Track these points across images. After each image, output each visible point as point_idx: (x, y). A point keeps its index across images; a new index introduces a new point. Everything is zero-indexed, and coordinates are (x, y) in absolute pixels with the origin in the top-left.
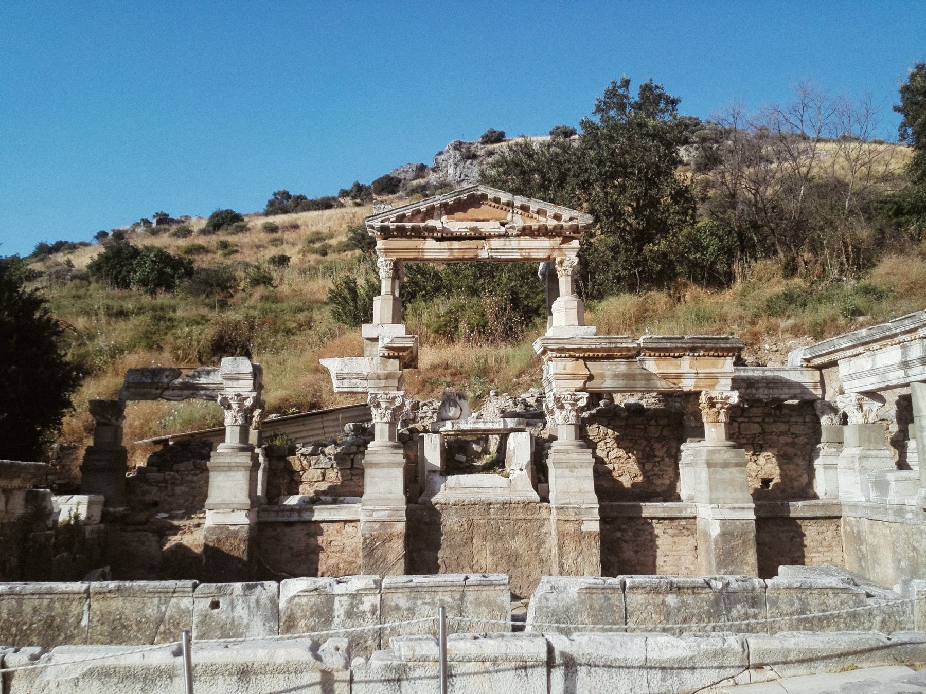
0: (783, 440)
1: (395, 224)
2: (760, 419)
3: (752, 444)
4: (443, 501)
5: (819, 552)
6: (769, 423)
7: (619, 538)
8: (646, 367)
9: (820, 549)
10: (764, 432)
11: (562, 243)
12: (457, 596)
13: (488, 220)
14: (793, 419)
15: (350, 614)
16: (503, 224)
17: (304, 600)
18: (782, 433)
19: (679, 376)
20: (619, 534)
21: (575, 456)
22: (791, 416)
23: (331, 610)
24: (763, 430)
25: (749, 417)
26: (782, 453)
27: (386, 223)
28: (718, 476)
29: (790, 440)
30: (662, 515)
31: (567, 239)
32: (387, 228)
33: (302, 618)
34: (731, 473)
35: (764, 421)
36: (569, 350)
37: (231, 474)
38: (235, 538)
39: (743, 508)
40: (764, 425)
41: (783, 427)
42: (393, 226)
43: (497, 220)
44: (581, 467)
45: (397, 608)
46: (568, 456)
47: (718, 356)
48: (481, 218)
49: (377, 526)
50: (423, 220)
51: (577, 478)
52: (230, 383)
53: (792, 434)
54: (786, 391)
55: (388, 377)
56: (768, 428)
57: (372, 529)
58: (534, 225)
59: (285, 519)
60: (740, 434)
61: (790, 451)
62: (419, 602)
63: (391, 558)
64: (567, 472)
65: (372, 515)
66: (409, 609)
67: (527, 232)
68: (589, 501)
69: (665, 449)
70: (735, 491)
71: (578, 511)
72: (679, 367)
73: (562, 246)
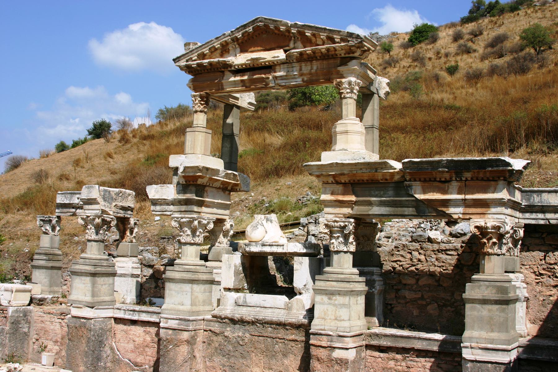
1: (195, 62)
7: (390, 368)
11: (341, 65)
20: (392, 363)
21: (334, 284)
28: (475, 313)
34: (489, 311)
36: (334, 176)
38: (85, 327)
42: (194, 64)
47: (488, 180)
49: (170, 332)
50: (222, 56)
51: (334, 305)
52: (86, 207)
55: (187, 202)
57: (167, 334)
63: (180, 359)
65: (167, 323)
67: (305, 57)
68: (342, 329)
70: (492, 331)
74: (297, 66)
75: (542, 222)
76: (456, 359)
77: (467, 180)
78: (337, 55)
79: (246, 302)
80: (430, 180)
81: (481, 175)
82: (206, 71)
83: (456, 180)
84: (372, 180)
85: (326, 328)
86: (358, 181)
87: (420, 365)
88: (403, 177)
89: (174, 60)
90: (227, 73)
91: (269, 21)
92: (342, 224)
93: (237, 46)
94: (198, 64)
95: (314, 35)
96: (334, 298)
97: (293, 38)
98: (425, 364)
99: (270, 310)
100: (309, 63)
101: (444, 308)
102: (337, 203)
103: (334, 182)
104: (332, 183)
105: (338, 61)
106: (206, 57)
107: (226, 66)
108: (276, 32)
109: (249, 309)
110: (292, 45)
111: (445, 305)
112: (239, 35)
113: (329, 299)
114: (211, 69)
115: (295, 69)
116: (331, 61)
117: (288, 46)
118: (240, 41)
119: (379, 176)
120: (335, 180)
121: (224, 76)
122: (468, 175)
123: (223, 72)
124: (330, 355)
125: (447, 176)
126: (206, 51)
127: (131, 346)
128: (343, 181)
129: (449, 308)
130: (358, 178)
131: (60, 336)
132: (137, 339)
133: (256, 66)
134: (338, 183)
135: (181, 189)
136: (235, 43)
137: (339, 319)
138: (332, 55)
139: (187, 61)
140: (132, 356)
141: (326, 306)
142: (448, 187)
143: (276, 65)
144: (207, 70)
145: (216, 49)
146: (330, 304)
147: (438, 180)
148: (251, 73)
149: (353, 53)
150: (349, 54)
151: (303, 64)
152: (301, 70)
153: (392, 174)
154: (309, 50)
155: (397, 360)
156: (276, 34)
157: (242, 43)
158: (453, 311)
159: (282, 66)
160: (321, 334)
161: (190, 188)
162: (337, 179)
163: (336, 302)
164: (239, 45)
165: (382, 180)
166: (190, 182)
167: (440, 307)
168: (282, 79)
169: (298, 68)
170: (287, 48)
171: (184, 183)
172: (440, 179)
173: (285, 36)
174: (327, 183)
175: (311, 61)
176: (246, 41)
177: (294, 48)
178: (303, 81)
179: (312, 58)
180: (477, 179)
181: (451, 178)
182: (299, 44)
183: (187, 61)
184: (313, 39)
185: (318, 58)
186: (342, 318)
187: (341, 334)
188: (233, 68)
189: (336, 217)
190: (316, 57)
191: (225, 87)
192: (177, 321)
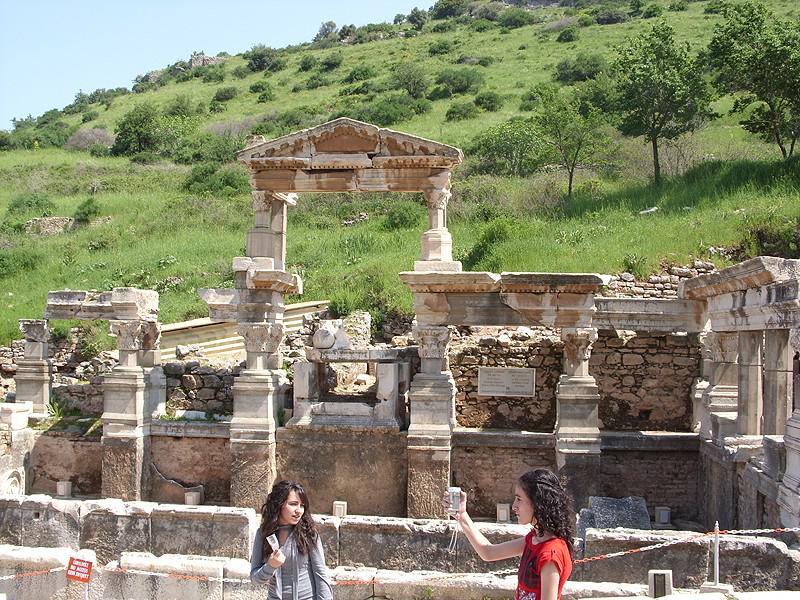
1: (264, 159)
2: (644, 350)
3: (633, 375)
5: (674, 484)
6: (653, 355)
8: (508, 303)
9: (674, 481)
10: (646, 363)
12: (208, 524)
13: (356, 152)
15: (129, 530)
17: (97, 517)
18: (666, 365)
19: (539, 313)
20: (479, 462)
22: (676, 347)
23: (115, 527)
24: (645, 361)
25: (633, 348)
26: (662, 384)
29: (672, 372)
30: (522, 446)
31: (437, 171)
33: (95, 530)
34: (581, 409)
35: (647, 352)
36: (429, 286)
37: (122, 394)
41: (665, 358)
44: (437, 401)
45: (163, 529)
48: (349, 150)
50: (293, 153)
53: (675, 365)
54: (669, 323)
56: (650, 359)
59: (173, 434)
60: (622, 365)
61: (670, 382)
62: (180, 526)
64: (422, 405)
66: (172, 531)
69: (545, 379)
72: (539, 303)
73: (430, 179)
74: (383, 172)
75: (607, 328)
81: (574, 289)
90: (300, 174)
94: (267, 162)
95: (404, 143)
107: (300, 165)
109: (329, 418)
110: (377, 151)
116: (421, 171)
119: (476, 287)
122: (562, 288)
124: (430, 458)
125: (542, 289)
127: (176, 465)
131: (74, 461)
132: (183, 458)
133: (336, 168)
134: (431, 292)
139: (252, 157)
140: (178, 475)
151: (390, 171)
152: (387, 177)
153: (489, 286)
154: (401, 159)
155: (484, 459)
160: (419, 439)
161: (260, 292)
178: (389, 187)
182: (386, 150)
183: (252, 157)
188: (309, 168)
189: (429, 325)
192: (252, 435)
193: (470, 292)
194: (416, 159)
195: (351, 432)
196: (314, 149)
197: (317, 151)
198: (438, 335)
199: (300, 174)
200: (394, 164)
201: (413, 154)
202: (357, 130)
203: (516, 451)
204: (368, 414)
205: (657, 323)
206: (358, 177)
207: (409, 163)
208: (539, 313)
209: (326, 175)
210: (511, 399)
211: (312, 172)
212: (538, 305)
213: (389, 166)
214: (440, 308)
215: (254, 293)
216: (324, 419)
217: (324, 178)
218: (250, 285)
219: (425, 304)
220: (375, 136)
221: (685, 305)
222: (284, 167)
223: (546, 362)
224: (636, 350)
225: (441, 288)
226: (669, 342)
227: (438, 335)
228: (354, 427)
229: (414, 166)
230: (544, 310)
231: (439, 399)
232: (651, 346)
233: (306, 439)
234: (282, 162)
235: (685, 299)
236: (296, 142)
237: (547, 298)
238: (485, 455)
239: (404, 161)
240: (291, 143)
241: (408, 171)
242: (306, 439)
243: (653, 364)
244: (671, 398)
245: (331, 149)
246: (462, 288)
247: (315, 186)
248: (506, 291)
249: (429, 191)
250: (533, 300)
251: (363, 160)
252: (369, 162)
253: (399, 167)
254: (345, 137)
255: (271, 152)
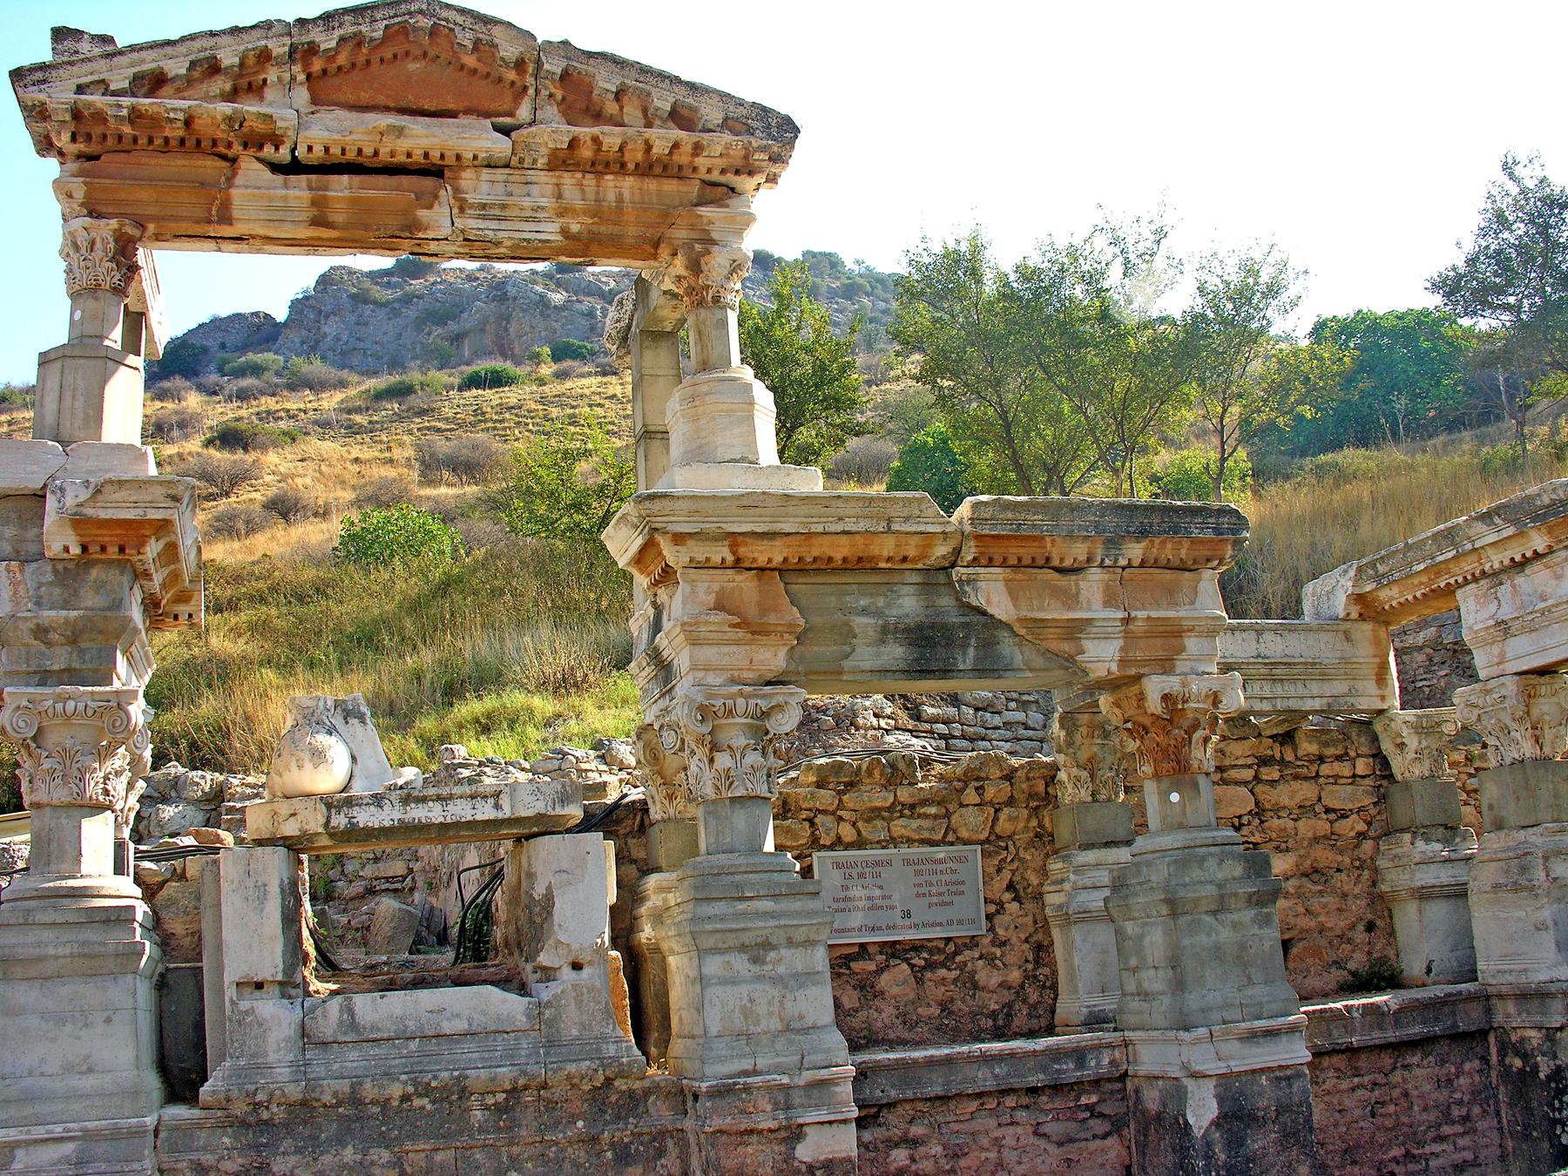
0: (1306, 827)
1: (127, 101)
4: (295, 1092)
10: (1259, 812)
14: (1325, 769)
16: (506, 131)
18: (1304, 809)
22: (1321, 759)
27: (96, 99)
29: (1322, 827)
32: (100, 117)
35: (1256, 777)
36: (734, 539)
39: (1271, 1034)
40: (1259, 789)
41: (1306, 791)
43: (487, 115)
44: (790, 943)
46: (741, 906)
50: (232, 96)
51: (777, 980)
53: (1328, 810)
58: (612, 138)
61: (1324, 856)
64: (740, 963)
67: (586, 153)
68: (818, 1058)
71: (783, 1097)
72: (1071, 599)
76: (1084, 1100)
77: (1129, 566)
78: (695, 169)
79: (353, 1026)
80: (1033, 565)
81: (1168, 552)
82: (158, 142)
83: (1101, 566)
84: (860, 559)
85: (762, 1063)
86: (815, 559)
87: (985, 1142)
88: (957, 552)
89: (18, 76)
90: (252, 171)
91: (460, 19)
92: (764, 704)
93: (302, 77)
94: (135, 116)
95: (618, 95)
96: (772, 955)
97: (531, 91)
98: (998, 1133)
99: (469, 1045)
100: (590, 180)
101: (929, 975)
102: (741, 634)
103: (730, 559)
104: (722, 566)
105: (693, 189)
106: (168, 89)
108: (470, 61)
109: (375, 1051)
110: (524, 113)
111: (930, 966)
112: (327, 42)
113: (755, 960)
114: (182, 141)
115: (535, 190)
116: (670, 186)
117: (511, 114)
118: (317, 65)
119: (886, 548)
120: (734, 553)
121: (235, 174)
122: (1135, 551)
123: (234, 161)
124: (789, 1157)
125: (1079, 551)
126: (176, 67)
128: (762, 561)
129: (942, 972)
130: (816, 552)
133: (384, 157)
134: (738, 565)
135: (50, 577)
136: (297, 68)
137: (796, 1025)
138: (680, 167)
139: (80, 89)
141: (744, 990)
142: (1077, 585)
143: (462, 168)
144: (167, 140)
145: (213, 68)
146: (758, 978)
147: (1056, 563)
148: (357, 179)
149: (751, 174)
150: (737, 172)
151: (568, 180)
155: (914, 1143)
156: (462, 67)
157: (325, 72)
158: (955, 980)
159: (486, 174)
162: (742, 551)
163: (781, 969)
164: (309, 77)
165: (889, 559)
166: (103, 549)
167: (918, 975)
168: (484, 218)
169: (549, 189)
170: (507, 120)
171: (75, 550)
172: (1062, 560)
173: (500, 80)
174: (705, 566)
175: (599, 174)
176: (339, 68)
177: (533, 122)
178: (564, 232)
179: (607, 164)
180: (1156, 565)
181: (1089, 560)
182: (551, 112)
184: (611, 108)
185: (631, 166)
186: (809, 1021)
187: (824, 1074)
188: (284, 155)
189: (733, 681)
190: (623, 165)
191: (236, 213)
193: (861, 564)
194: (663, 138)
195: (464, 1093)
196: (302, 95)
197: (315, 101)
198: (765, 715)
199: (252, 171)
200: (586, 153)
201: (649, 125)
202: (465, 38)
203: (1010, 1101)
204: (522, 1021)
205: (1291, 689)
206: (457, 190)
207: (635, 156)
208: (1075, 630)
209: (345, 178)
210: (916, 947)
211: (294, 167)
212: (1069, 609)
213: (563, 161)
214: (772, 619)
215: (70, 573)
216: (353, 1059)
217: (341, 186)
218: (59, 539)
219: (719, 607)
220: (520, 65)
221: (1347, 636)
222: (192, 141)
223: (1003, 826)
224: (1233, 774)
225: (775, 553)
226: (1309, 747)
227: (765, 715)
228: (478, 1076)
229: (649, 168)
230: (1089, 621)
231: (799, 936)
232: (1264, 761)
233: (287, 1144)
234: (188, 123)
235: (1347, 618)
236: (242, 65)
237: (1093, 583)
238: (917, 1130)
239: (621, 149)
240: (228, 59)
241: (629, 182)
242: (287, 1144)
243: (1277, 810)
244: (1332, 901)
245: (365, 97)
246: (840, 550)
247: (304, 216)
248: (975, 562)
249: (698, 247)
250: (1057, 593)
251: (478, 138)
252: (501, 146)
253: (604, 165)
254: (413, 66)
255: (156, 82)
